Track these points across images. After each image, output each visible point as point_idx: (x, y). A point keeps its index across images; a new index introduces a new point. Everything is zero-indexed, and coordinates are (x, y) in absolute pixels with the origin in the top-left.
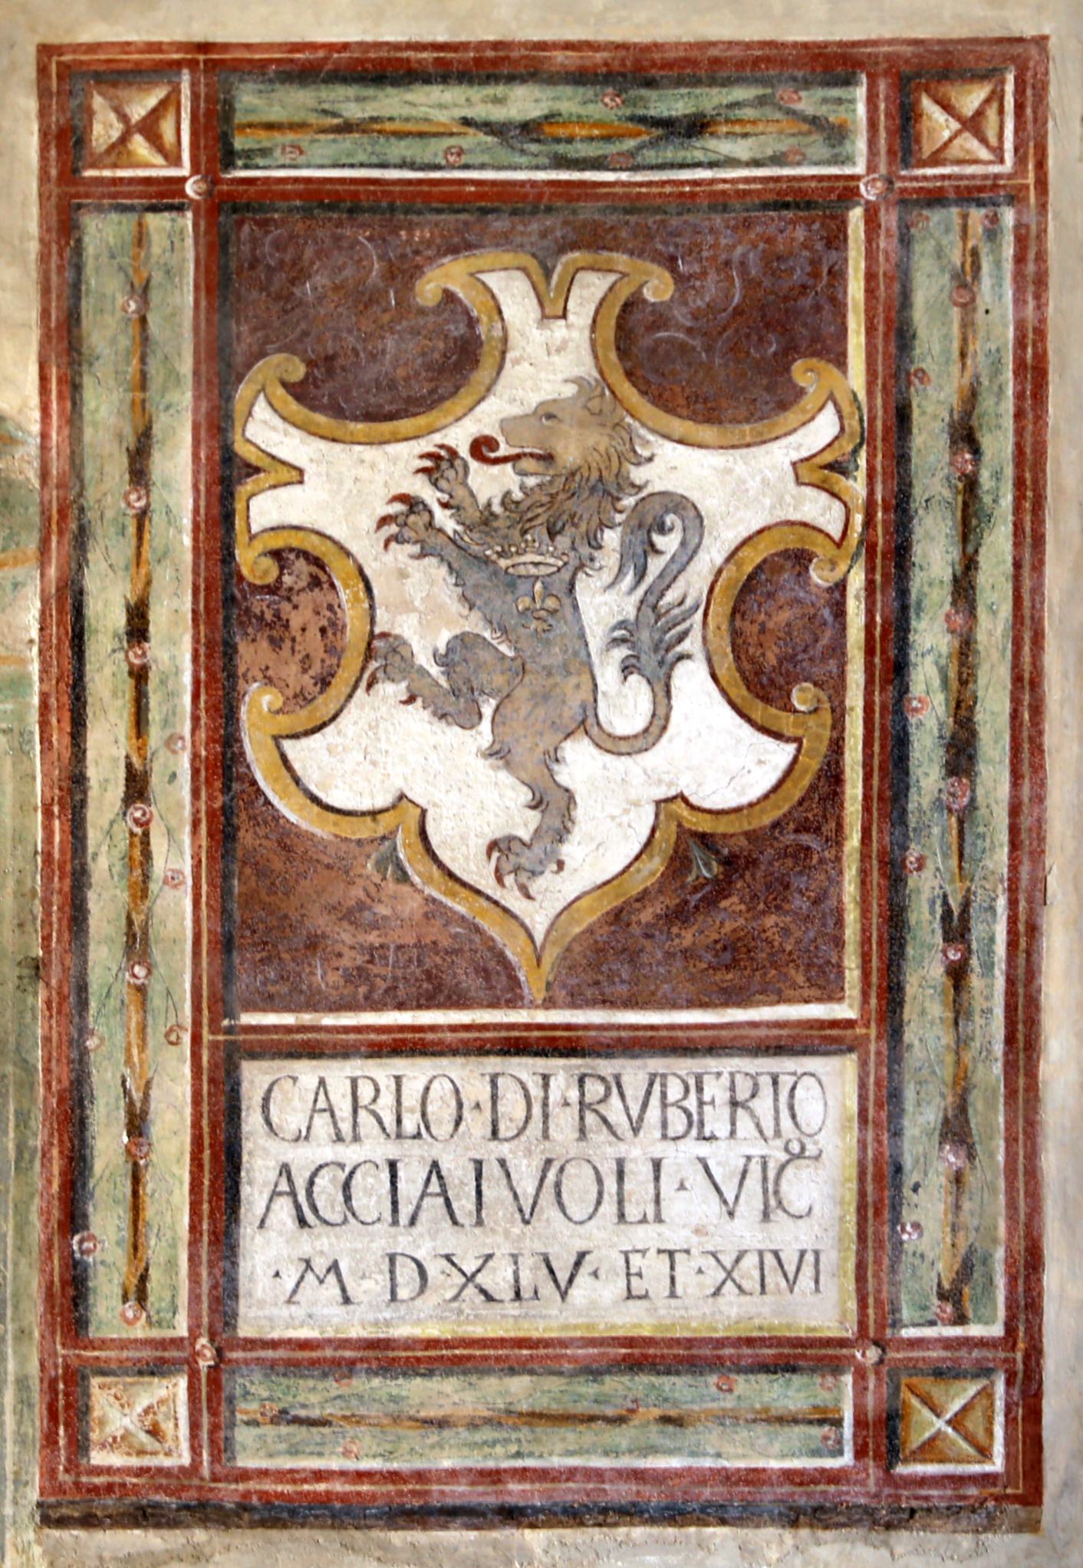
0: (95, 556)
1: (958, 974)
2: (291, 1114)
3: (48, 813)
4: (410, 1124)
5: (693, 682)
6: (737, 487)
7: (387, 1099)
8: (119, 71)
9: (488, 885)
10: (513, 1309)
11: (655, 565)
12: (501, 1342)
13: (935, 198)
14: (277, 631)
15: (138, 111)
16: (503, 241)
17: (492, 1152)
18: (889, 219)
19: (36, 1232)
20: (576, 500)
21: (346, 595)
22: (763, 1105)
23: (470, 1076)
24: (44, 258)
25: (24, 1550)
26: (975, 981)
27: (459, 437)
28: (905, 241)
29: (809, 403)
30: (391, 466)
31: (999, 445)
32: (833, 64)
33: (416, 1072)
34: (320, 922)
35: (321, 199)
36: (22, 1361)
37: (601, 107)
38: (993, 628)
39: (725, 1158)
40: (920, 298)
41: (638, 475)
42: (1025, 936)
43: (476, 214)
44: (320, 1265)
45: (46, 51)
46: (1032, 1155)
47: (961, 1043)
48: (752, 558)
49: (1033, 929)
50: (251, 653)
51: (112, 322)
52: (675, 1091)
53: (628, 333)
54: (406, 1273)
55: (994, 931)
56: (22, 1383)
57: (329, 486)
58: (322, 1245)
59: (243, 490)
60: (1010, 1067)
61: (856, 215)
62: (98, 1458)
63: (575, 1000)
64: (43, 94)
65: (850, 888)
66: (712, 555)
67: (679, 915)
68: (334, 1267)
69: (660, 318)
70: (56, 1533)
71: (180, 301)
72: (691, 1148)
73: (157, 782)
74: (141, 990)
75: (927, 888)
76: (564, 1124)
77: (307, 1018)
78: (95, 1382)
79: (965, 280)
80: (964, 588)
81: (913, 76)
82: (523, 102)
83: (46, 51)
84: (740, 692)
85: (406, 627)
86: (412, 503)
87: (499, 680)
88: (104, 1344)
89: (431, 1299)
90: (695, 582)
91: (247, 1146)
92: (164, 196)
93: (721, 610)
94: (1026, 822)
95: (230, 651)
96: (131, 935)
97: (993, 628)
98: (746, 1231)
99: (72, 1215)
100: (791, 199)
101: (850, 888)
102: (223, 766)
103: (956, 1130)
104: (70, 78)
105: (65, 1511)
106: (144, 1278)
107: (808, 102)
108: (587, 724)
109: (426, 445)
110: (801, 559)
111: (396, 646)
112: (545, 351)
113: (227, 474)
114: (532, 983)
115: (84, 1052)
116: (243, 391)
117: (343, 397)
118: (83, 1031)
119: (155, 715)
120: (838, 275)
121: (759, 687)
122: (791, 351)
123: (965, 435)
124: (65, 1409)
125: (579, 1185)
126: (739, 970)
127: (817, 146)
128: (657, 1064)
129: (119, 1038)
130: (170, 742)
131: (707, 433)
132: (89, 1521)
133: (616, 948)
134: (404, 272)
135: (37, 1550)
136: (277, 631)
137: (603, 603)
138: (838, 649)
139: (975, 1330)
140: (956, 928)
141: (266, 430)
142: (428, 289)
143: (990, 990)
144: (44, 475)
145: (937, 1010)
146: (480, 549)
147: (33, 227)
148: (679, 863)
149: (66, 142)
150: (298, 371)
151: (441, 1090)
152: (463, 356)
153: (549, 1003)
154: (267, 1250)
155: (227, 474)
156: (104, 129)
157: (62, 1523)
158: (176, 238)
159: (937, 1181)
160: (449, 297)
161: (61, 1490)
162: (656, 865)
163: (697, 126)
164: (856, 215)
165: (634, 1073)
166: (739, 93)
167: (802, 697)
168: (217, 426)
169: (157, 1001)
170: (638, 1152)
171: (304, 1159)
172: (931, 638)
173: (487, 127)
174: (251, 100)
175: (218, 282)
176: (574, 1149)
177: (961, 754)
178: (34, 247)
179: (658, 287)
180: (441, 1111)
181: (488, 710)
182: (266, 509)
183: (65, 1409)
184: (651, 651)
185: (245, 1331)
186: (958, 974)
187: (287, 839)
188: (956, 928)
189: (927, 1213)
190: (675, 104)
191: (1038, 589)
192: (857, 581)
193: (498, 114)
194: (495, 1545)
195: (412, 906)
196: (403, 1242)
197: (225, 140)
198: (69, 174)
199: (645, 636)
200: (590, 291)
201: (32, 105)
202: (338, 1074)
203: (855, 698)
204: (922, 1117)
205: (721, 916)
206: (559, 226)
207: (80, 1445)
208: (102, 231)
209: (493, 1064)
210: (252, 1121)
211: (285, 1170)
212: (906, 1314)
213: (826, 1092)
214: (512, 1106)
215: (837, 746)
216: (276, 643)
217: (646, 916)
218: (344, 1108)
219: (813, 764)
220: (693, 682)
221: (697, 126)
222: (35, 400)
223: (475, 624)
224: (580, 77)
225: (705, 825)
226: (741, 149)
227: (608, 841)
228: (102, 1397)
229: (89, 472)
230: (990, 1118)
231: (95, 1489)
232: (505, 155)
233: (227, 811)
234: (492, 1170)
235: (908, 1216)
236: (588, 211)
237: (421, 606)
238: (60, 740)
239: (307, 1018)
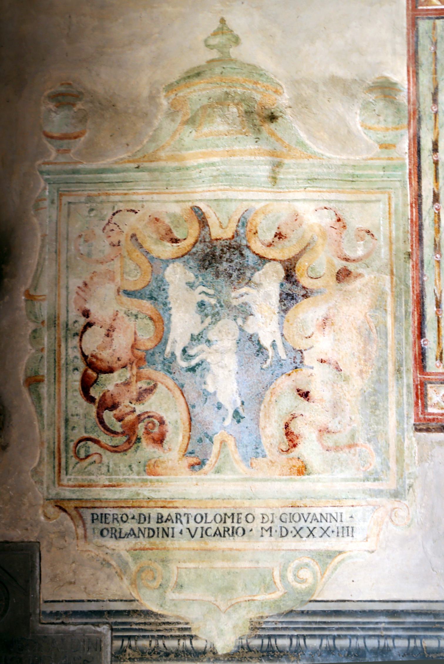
25: (410, 439)
51: (427, 53)
56: (408, 386)
62: (430, 410)
70: (419, 434)
78: (429, 386)
88: (430, 374)
99: (421, 334)
105: (421, 427)
106: (441, 353)
124: (421, 394)
135: (414, 439)
144: (409, 101)
157: (420, 430)
161: (420, 420)
183: (421, 394)
207: (425, 406)
208: (424, 25)
222: (406, 78)
228: (431, 390)
229: (421, 100)
231: (429, 420)
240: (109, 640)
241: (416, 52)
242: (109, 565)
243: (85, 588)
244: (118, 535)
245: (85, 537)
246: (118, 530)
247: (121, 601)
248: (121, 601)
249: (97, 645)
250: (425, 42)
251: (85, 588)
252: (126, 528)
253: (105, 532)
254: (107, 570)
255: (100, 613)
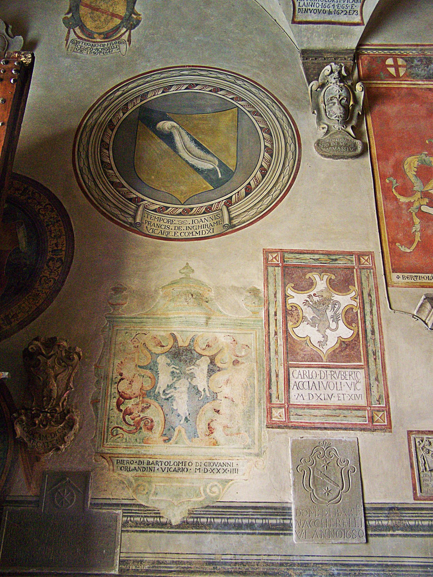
0: (270, 306)
1: (375, 359)
2: (296, 375)
3: (265, 336)
4: (310, 377)
5: (340, 322)
6: (345, 300)
7: (307, 373)
8: (272, 252)
9: (318, 347)
10: (324, 401)
11: (335, 309)
12: (323, 405)
13: (363, 269)
14: (292, 315)
15: (274, 256)
16: (315, 272)
17: (320, 380)
18: (359, 270)
19: (265, 389)
20: (325, 302)
21: (300, 311)
22: (353, 375)
23: (317, 370)
24: (264, 271)
25: (264, 431)
26: (377, 360)
27: (312, 293)
28: (360, 273)
29: (351, 291)
30: (304, 296)
31: (374, 296)
32: (351, 254)
33: (311, 370)
34: (298, 351)
35: (295, 266)
36: (264, 406)
37: (326, 257)
38: (375, 318)
39: (349, 382)
40: (363, 279)
41: (333, 298)
42: (383, 355)
43: (313, 268)
44: (300, 395)
45: (264, 249)
46: (386, 383)
47: (376, 368)
48: (346, 308)
49: (384, 354)
50: (289, 318)
51: (272, 279)
52: (342, 373)
53: (330, 281)
54: (311, 396)
55: (379, 354)
56: (264, 409)
57: (297, 299)
58: (300, 392)
59: (287, 299)
60: (383, 371)
61: (355, 270)
62: (273, 419)
63: (329, 362)
64: (264, 254)
65: (361, 348)
66: (342, 308)
67: (342, 351)
68: (302, 395)
69: (334, 281)
70: (268, 429)
71: (279, 277)
72: (345, 381)
73: (278, 333)
74: (277, 359)
75: (370, 349)
76: (329, 377)
77: (297, 363)
78: (273, 409)
79: (368, 278)
80: (371, 312)
81: (360, 255)
82: (317, 257)
83: (264, 249)
84: (346, 324)
85: (307, 315)
86: (307, 301)
87: (318, 322)
88: (274, 404)
89: (314, 400)
90: (340, 311)
91: (291, 379)
92: (277, 265)
93: (343, 314)
94: (381, 341)
95: (286, 317)
96: (276, 352)
97: (375, 318)
98: (352, 392)
100: (348, 268)
101: (361, 348)
102: (286, 331)
103: (377, 379)
104: (266, 252)
105: (269, 426)
106: (278, 396)
107: (348, 257)
108: (329, 327)
109: (308, 294)
110: (352, 309)
111: (306, 317)
112: (321, 284)
113: (285, 297)
114: (324, 359)
115: (270, 366)
116: (287, 288)
117: (298, 288)
118: (270, 363)
119: (278, 325)
120: (353, 276)
121: (349, 323)
122: (349, 285)
123: (370, 295)
124: (269, 413)
125: (331, 385)
126: (349, 358)
127: (349, 262)
128: (340, 370)
129: (275, 365)
130: (280, 328)
131: (340, 294)
132: (272, 428)
133: (334, 355)
134: (305, 275)
135: (266, 431)
136: (292, 315)
137: (330, 313)
138: (357, 319)
139: (381, 405)
140: (374, 354)
141: (290, 292)
142: (307, 277)
143: (379, 361)
144: (264, 296)
145: (373, 364)
146: (315, 307)
147: (263, 268)
148: (341, 345)
149: (266, 259)
150: (293, 285)
151: (314, 372)
152: (311, 284)
153: (326, 362)
154: (294, 392)
155: (285, 297)
156: (270, 258)
157: (269, 428)
158: (279, 270)
159: (375, 386)
160: (310, 277)
161: (269, 423)
162: (338, 345)
163: (336, 260)
164: (355, 270)
165: (337, 371)
166: (340, 256)
167: (354, 325)
168: (284, 291)
169: (279, 360)
170: (338, 381)
171: (298, 381)
172: (368, 318)
173: (313, 259)
174: (286, 255)
175: (284, 275)
176: (331, 380)
177: (373, 332)
178: (263, 271)
179: (333, 277)
180: (314, 375)
181: (317, 325)
182: (290, 301)
183: (269, 413)
184: (336, 319)
185: (291, 403)
186: (375, 359)
187: (293, 339)
188: (374, 354)
189: (374, 389)
190: (334, 257)
191: (380, 313)
192: (359, 311)
193: (314, 258)
194: (324, 433)
195: (309, 349)
196: (310, 392)
197: (284, 259)
198: (267, 263)
199: (335, 317)
200: (326, 277)
201: (262, 255)
202: (301, 370)
203: (360, 325)
204: (373, 378)
205: (347, 352)
206: (322, 270)
207: (271, 417)
208: (270, 269)
209: (320, 369)
210: (291, 376)
211: (295, 382)
212: (373, 403)
213: (361, 374)
214: (323, 375)
215: (358, 331)
216: (292, 317)
217: (337, 351)
218: (302, 374)
219: (356, 333)
220: (340, 322)
221: (336, 260)
222: (263, 288)
223: (315, 315)
224: (322, 254)
225: (343, 340)
226: (341, 262)
227: (332, 342)
228: (274, 411)
229: (270, 296)
230: (381, 378)
231: (273, 423)
232: (315, 262)
233: (287, 337)
234: (321, 383)
235: (372, 390)
236: (325, 268)
237: (309, 313)
238: (267, 327)
239: (297, 363)
240: (121, 517)
241: (267, 278)
242: (124, 483)
243: (111, 493)
244: (128, 470)
245: (113, 470)
246: (129, 467)
247: (128, 499)
248: (128, 499)
249: (116, 519)
250: (270, 274)
251: (111, 493)
252: (133, 466)
253: (123, 468)
254: (122, 485)
255: (117, 505)
